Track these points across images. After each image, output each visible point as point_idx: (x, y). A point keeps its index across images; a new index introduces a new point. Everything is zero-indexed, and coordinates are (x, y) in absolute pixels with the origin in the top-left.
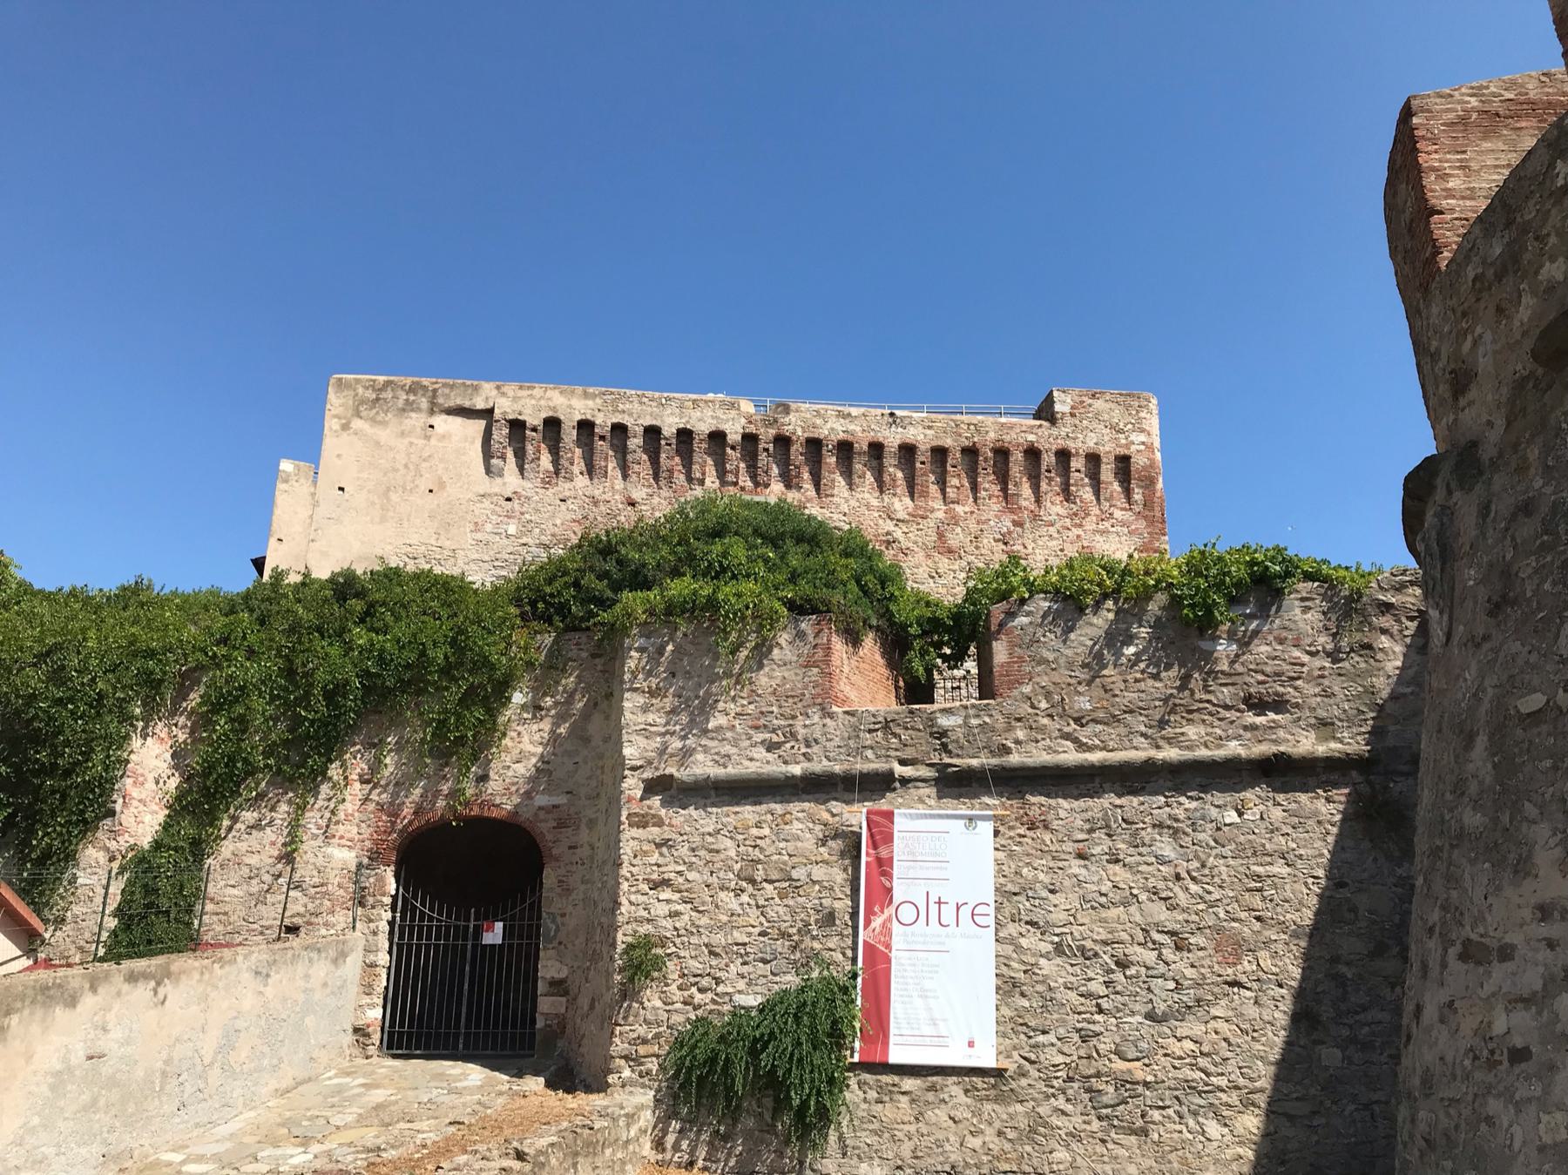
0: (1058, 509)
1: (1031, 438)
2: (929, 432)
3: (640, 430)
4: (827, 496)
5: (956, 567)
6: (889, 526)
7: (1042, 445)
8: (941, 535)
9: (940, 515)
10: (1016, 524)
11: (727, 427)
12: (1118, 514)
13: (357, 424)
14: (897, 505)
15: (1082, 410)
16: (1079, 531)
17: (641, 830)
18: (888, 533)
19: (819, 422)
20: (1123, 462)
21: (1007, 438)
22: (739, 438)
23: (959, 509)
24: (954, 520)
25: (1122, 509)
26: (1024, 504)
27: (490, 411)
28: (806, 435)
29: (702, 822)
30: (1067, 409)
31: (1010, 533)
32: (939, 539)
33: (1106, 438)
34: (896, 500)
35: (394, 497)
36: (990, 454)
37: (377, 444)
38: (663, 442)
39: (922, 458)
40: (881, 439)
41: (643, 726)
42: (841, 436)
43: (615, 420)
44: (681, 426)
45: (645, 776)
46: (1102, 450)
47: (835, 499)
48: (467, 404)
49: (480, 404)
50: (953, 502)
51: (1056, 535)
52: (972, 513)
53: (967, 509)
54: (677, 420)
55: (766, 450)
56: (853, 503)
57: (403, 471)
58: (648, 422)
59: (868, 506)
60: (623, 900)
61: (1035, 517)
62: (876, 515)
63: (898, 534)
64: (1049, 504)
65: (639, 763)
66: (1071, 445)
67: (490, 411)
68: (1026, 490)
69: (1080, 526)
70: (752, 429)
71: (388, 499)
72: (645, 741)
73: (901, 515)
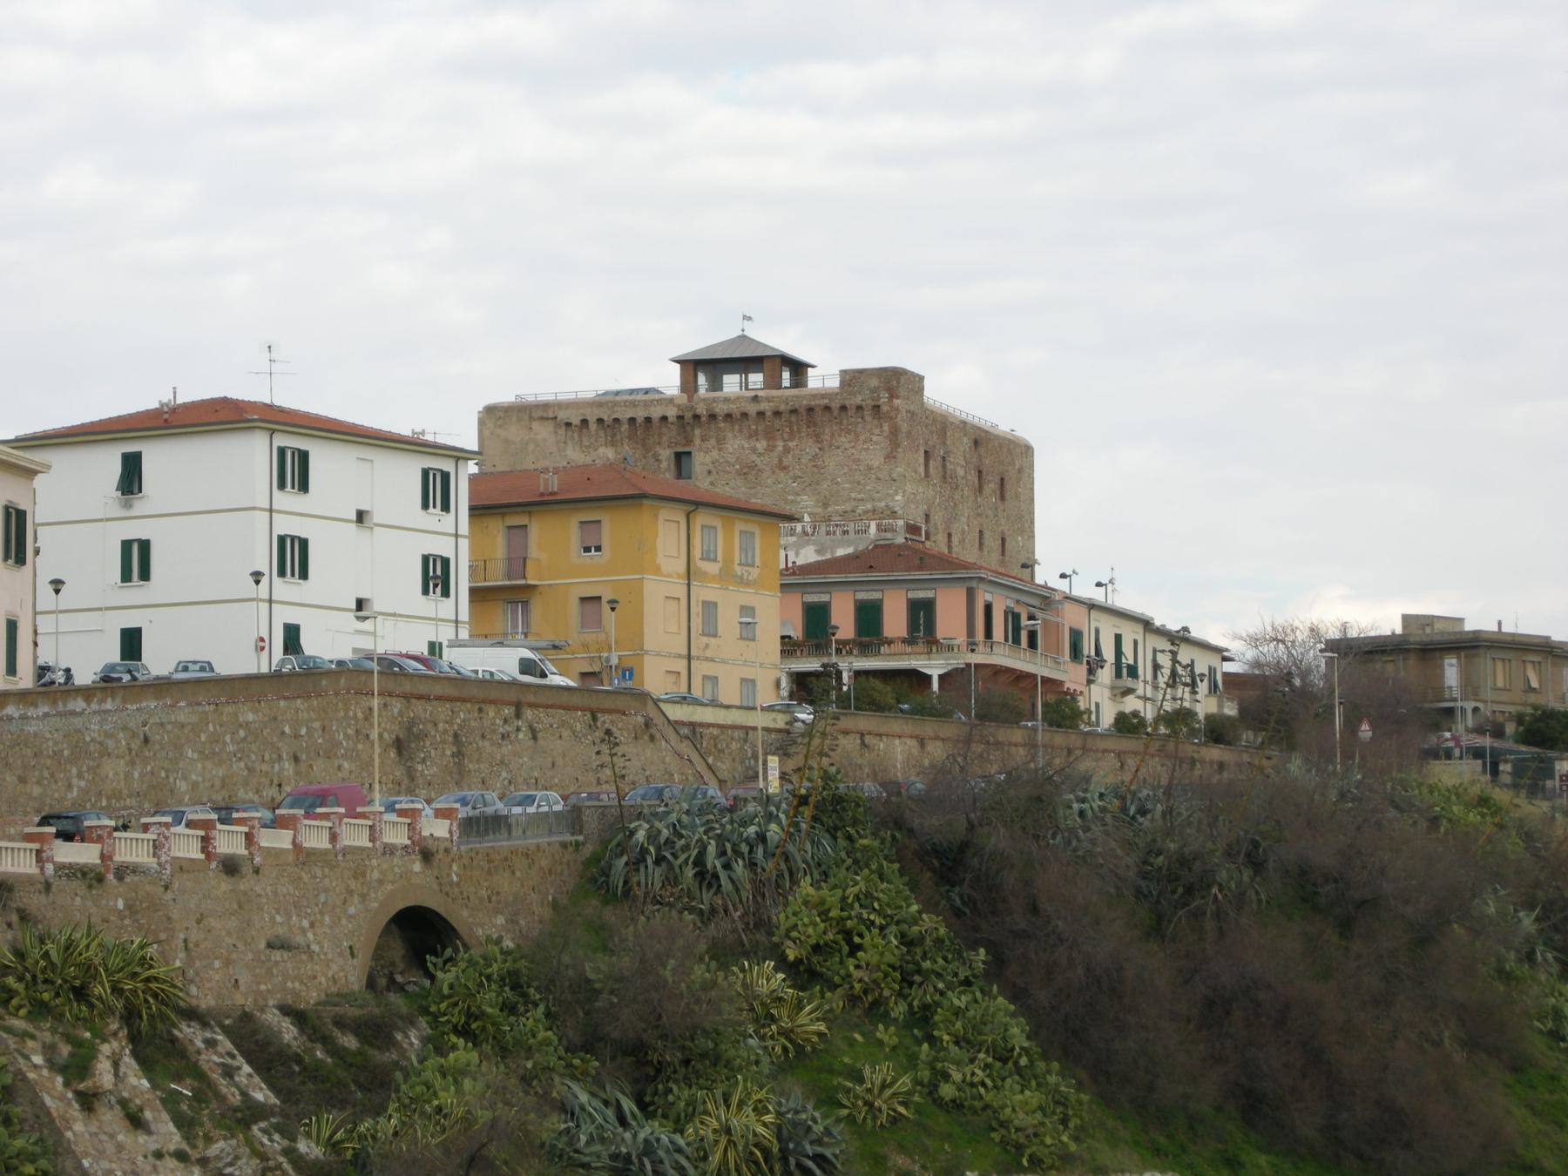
0: (843, 439)
1: (827, 401)
2: (771, 404)
3: (626, 422)
6: (754, 457)
8: (780, 460)
9: (781, 448)
10: (820, 449)
12: (875, 438)
13: (498, 431)
14: (758, 445)
16: (854, 451)
20: (877, 408)
21: (813, 403)
22: (675, 419)
24: (787, 450)
27: (556, 418)
31: (816, 455)
42: (726, 412)
48: (545, 415)
49: (551, 415)
53: (795, 443)
59: (743, 448)
66: (847, 403)
67: (556, 418)
69: (853, 447)
70: (680, 413)
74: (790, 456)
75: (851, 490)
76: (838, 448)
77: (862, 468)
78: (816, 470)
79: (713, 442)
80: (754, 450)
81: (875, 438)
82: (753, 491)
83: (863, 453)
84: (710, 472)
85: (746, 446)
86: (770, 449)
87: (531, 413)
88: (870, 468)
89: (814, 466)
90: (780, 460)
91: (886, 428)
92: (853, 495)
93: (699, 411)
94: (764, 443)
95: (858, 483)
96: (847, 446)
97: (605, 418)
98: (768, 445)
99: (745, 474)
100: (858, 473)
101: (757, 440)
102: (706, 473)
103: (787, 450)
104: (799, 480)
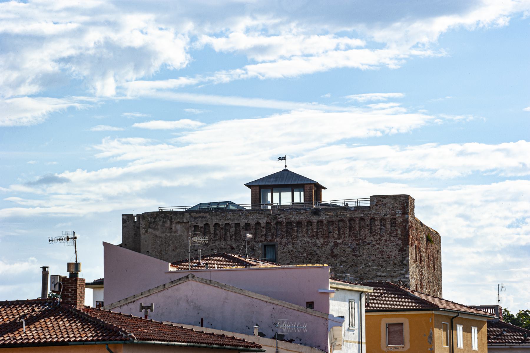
0: (372, 239)
1: (362, 215)
2: (327, 217)
3: (233, 225)
4: (294, 241)
6: (315, 249)
8: (332, 251)
9: (332, 244)
11: (261, 221)
12: (392, 239)
14: (318, 242)
18: (315, 251)
23: (339, 241)
31: (355, 248)
32: (331, 252)
33: (388, 213)
35: (163, 253)
37: (156, 236)
43: (226, 223)
44: (246, 222)
50: (336, 239)
51: (370, 248)
52: (343, 242)
53: (341, 241)
57: (165, 244)
58: (236, 222)
61: (364, 242)
64: (368, 237)
71: (162, 254)
73: (319, 245)
74: (338, 248)
75: (378, 270)
76: (369, 244)
77: (384, 257)
78: (355, 258)
80: (315, 244)
86: (325, 244)
87: (171, 219)
88: (389, 257)
89: (354, 255)
90: (332, 251)
91: (399, 232)
92: (379, 274)
94: (322, 240)
95: (382, 266)
96: (375, 243)
97: (221, 223)
98: (324, 242)
99: (310, 259)
100: (382, 260)
101: (317, 238)
103: (336, 244)
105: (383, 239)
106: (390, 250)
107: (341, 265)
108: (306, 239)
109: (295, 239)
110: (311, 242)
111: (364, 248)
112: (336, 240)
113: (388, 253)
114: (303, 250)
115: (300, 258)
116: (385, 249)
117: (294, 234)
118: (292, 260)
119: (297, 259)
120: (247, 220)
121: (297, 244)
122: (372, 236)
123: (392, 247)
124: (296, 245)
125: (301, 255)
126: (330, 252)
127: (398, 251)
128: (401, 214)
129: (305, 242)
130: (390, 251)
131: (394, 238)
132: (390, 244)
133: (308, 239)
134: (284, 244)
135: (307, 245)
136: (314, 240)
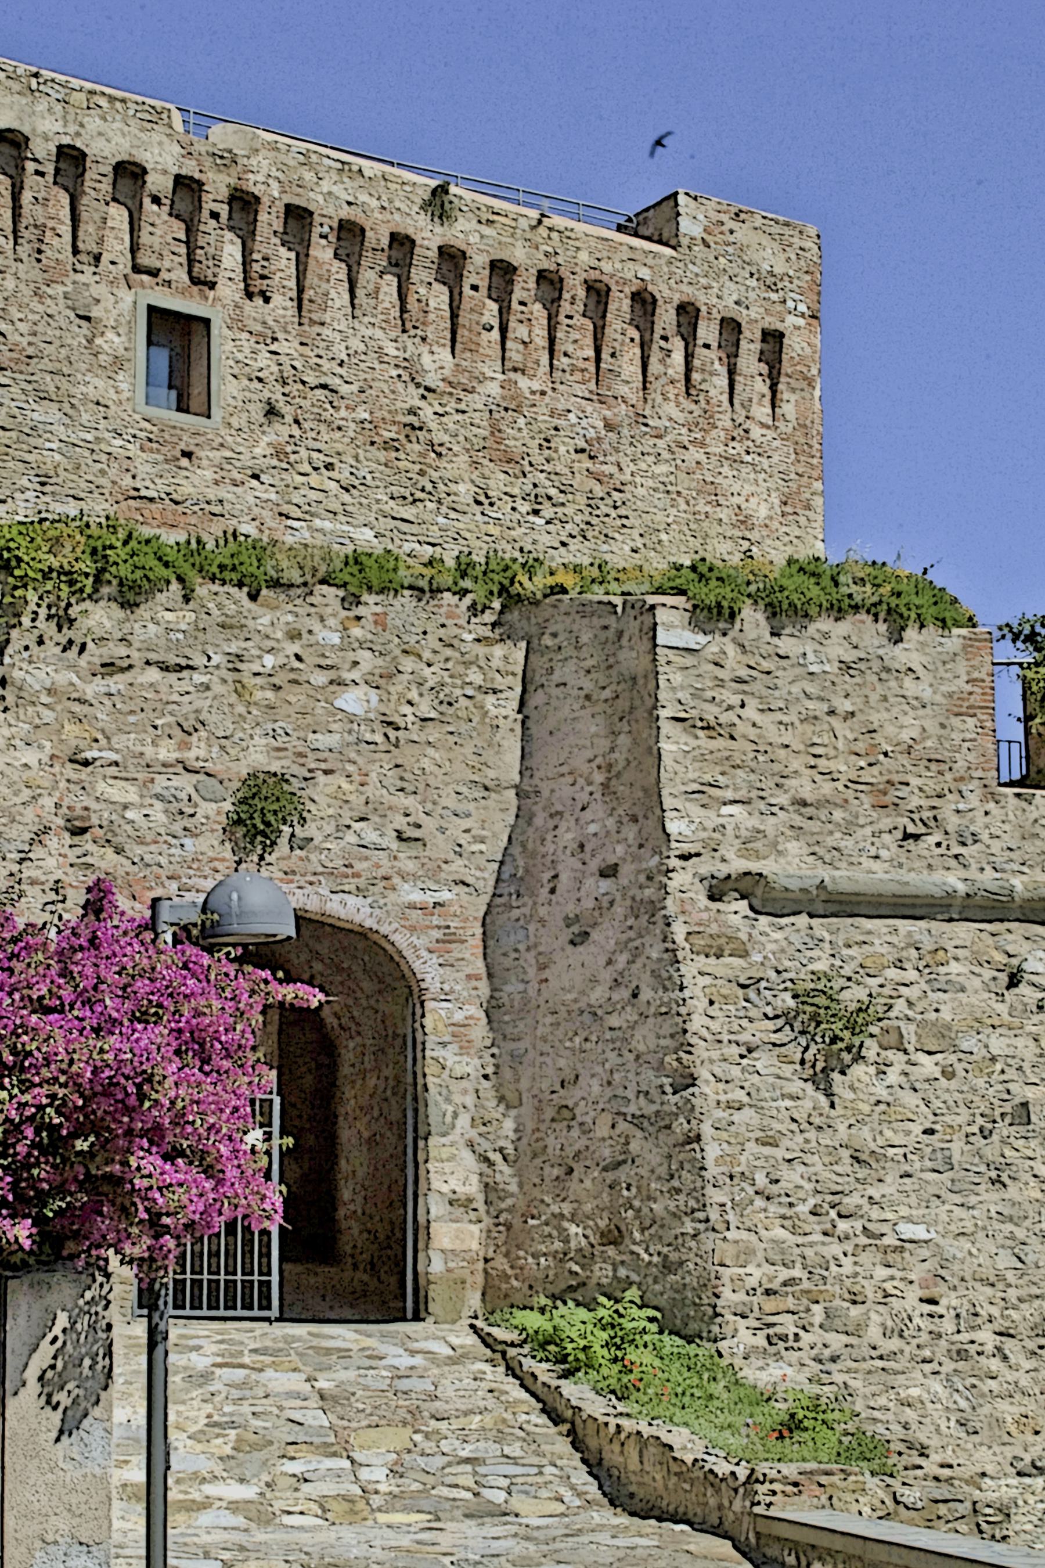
0: (670, 409)
2: (487, 231)
4: (312, 322)
5: (516, 491)
6: (412, 397)
7: (661, 290)
9: (493, 389)
11: (146, 158)
14: (426, 360)
15: (719, 238)
17: (712, 960)
18: (412, 412)
19: (309, 176)
20: (773, 338)
25: (763, 425)
26: (623, 390)
28: (287, 199)
29: (809, 954)
30: (697, 231)
34: (424, 349)
36: (581, 293)
38: (30, 166)
39: (473, 279)
40: (410, 231)
41: (696, 787)
44: (66, 140)
45: (705, 870)
46: (743, 316)
47: (326, 332)
52: (543, 393)
53: (536, 386)
54: (58, 127)
55: (215, 215)
56: (356, 344)
60: (703, 1073)
62: (394, 373)
63: (427, 413)
64: (659, 399)
65: (692, 848)
66: (701, 299)
68: (629, 366)
69: (703, 444)
70: (189, 168)
72: (702, 812)
77: (723, 514)
79: (282, 304)
81: (756, 432)
82: (408, 512)
83: (726, 470)
84: (272, 412)
85: (391, 349)
90: (496, 430)
93: (254, 184)
102: (257, 412)
104: (548, 511)
105: (719, 424)
106: (748, 489)
107: (536, 512)
108: (369, 332)
109: (315, 317)
110: (396, 353)
111: (640, 448)
112: (512, 375)
113: (736, 500)
114: (354, 388)
115: (339, 428)
116: (727, 479)
117: (316, 281)
118: (296, 432)
119: (323, 428)
120: (72, 129)
121: (323, 344)
122: (672, 396)
123: (752, 476)
124: (322, 353)
125: (343, 413)
126: (486, 433)
127: (777, 502)
128: (803, 315)
129: (362, 347)
130: (744, 493)
131: (764, 431)
132: (748, 458)
133: (379, 334)
134: (259, 328)
135: (377, 365)
136: (410, 348)
